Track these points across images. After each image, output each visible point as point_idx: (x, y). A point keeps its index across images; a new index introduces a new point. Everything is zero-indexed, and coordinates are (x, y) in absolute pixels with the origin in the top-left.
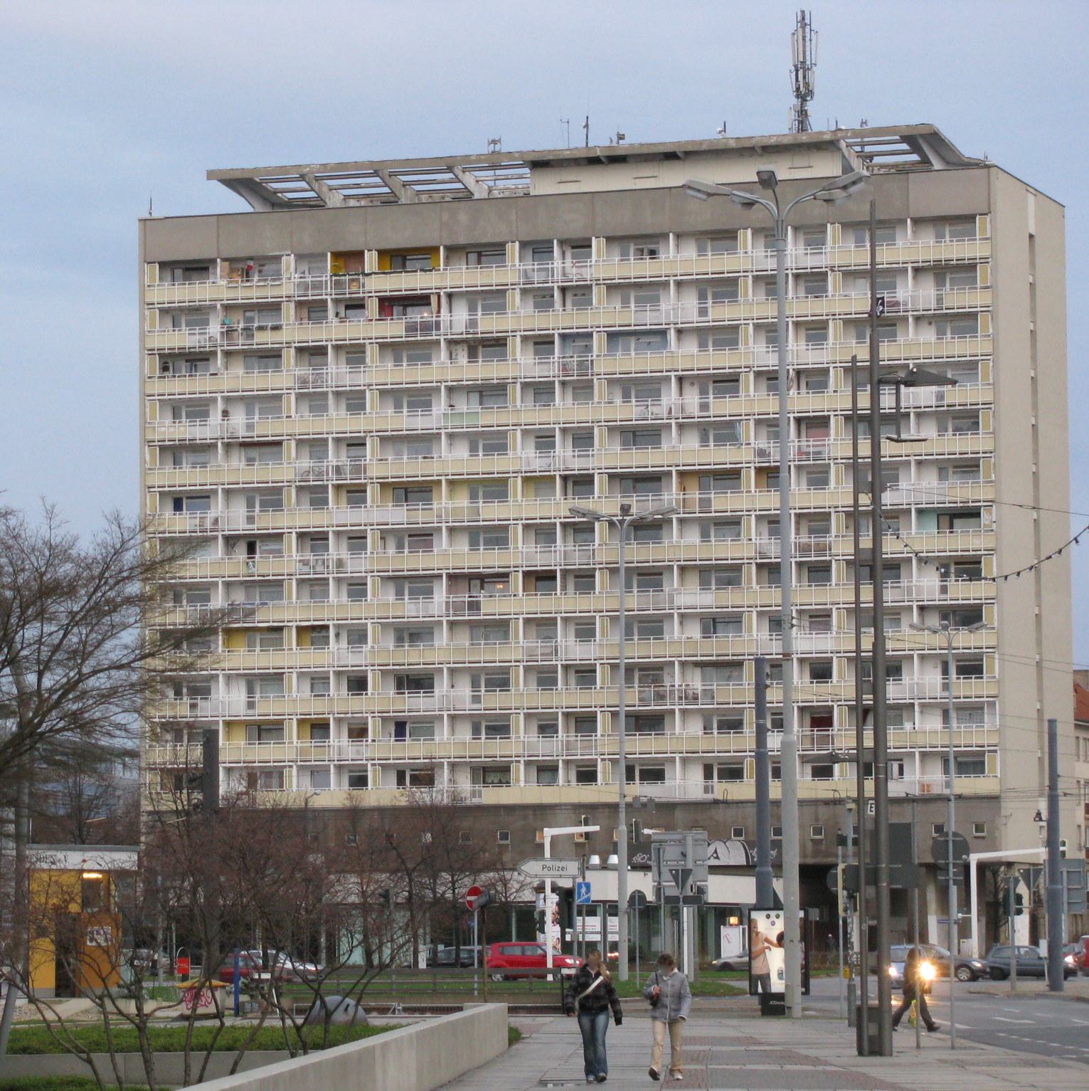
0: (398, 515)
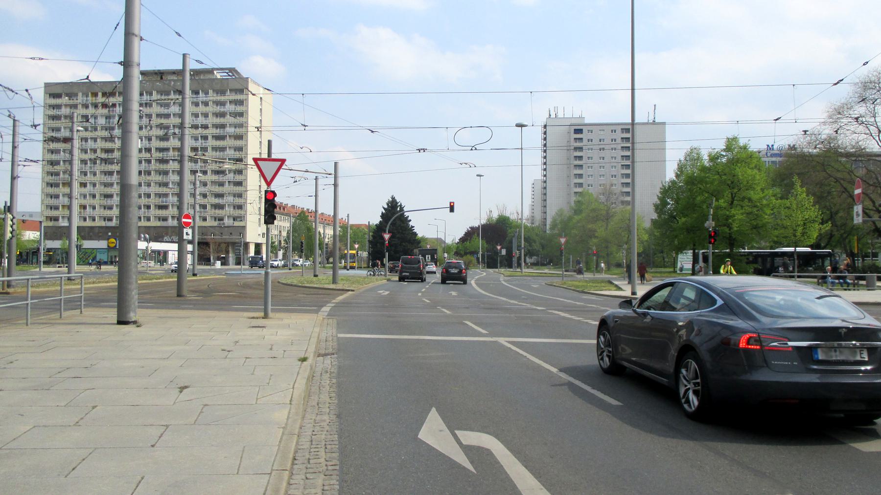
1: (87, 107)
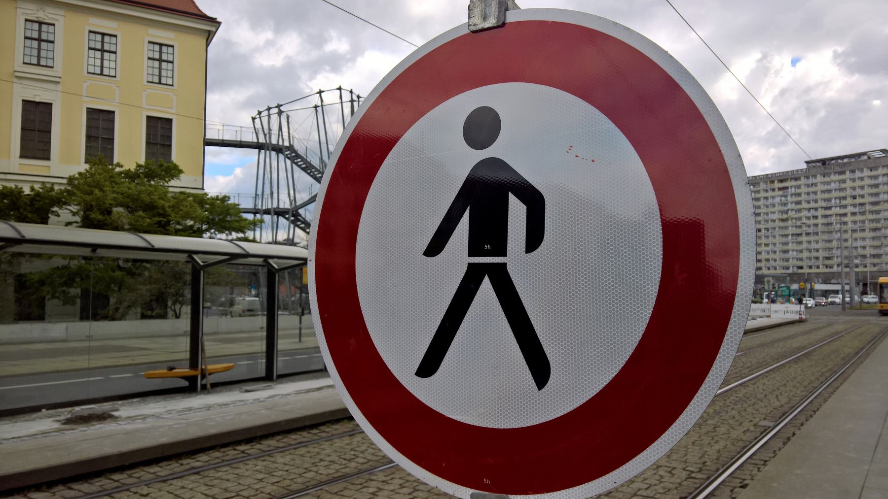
0: (782, 224)
1: (767, 191)
